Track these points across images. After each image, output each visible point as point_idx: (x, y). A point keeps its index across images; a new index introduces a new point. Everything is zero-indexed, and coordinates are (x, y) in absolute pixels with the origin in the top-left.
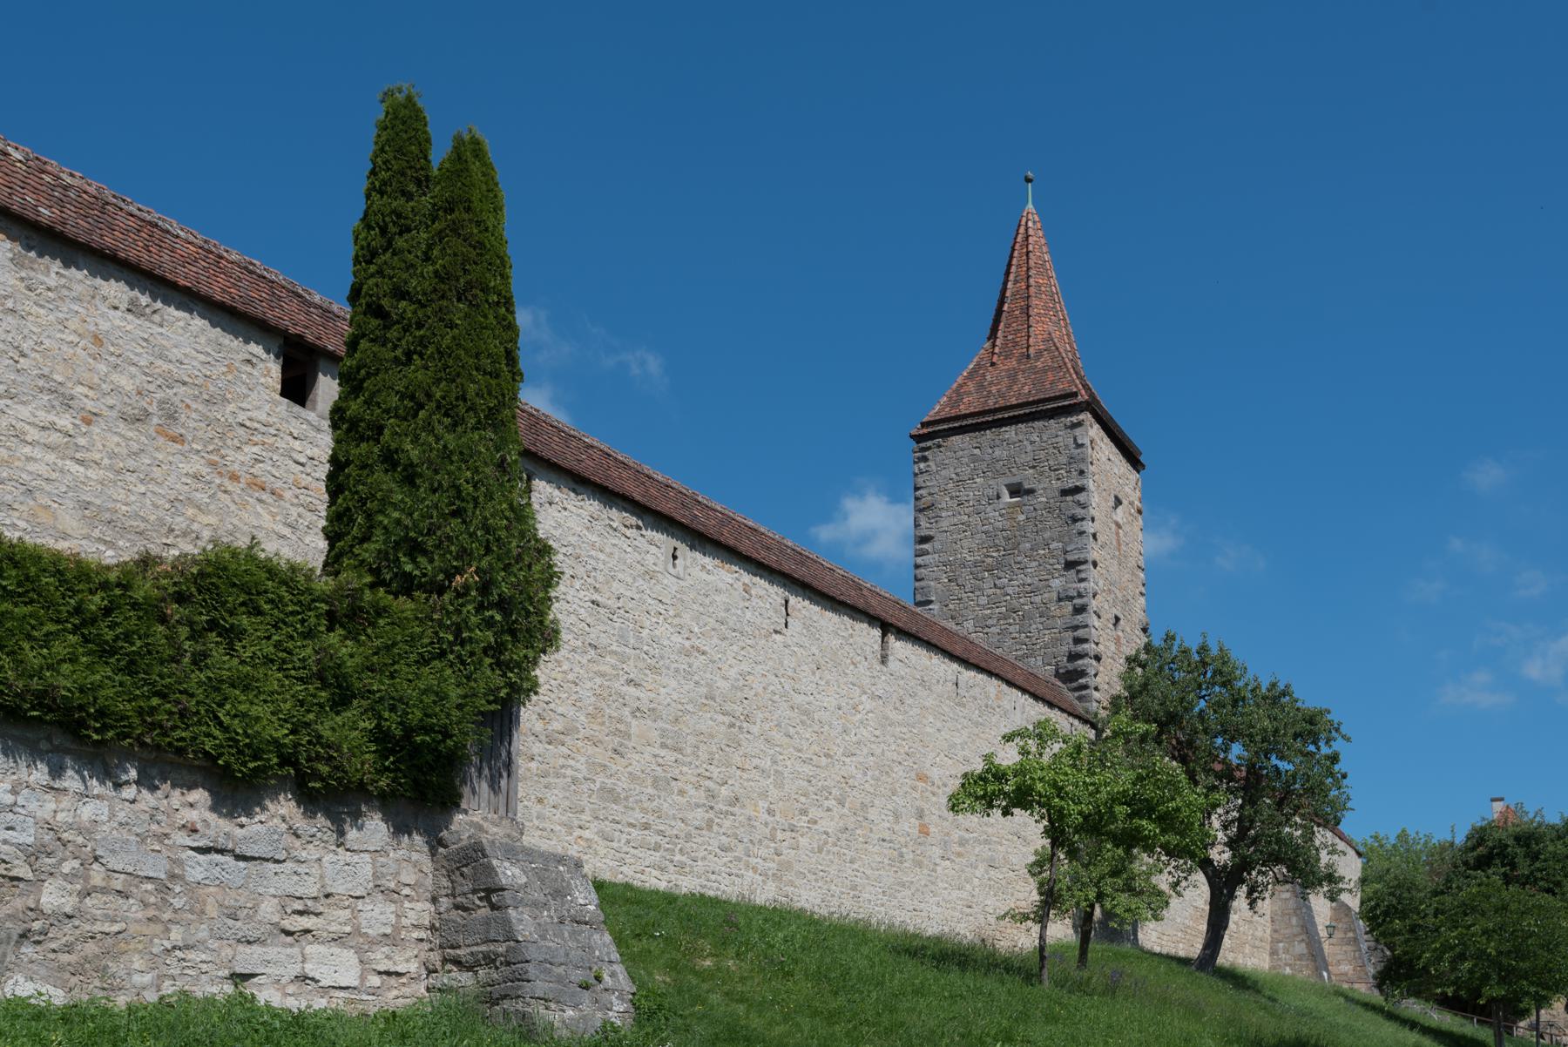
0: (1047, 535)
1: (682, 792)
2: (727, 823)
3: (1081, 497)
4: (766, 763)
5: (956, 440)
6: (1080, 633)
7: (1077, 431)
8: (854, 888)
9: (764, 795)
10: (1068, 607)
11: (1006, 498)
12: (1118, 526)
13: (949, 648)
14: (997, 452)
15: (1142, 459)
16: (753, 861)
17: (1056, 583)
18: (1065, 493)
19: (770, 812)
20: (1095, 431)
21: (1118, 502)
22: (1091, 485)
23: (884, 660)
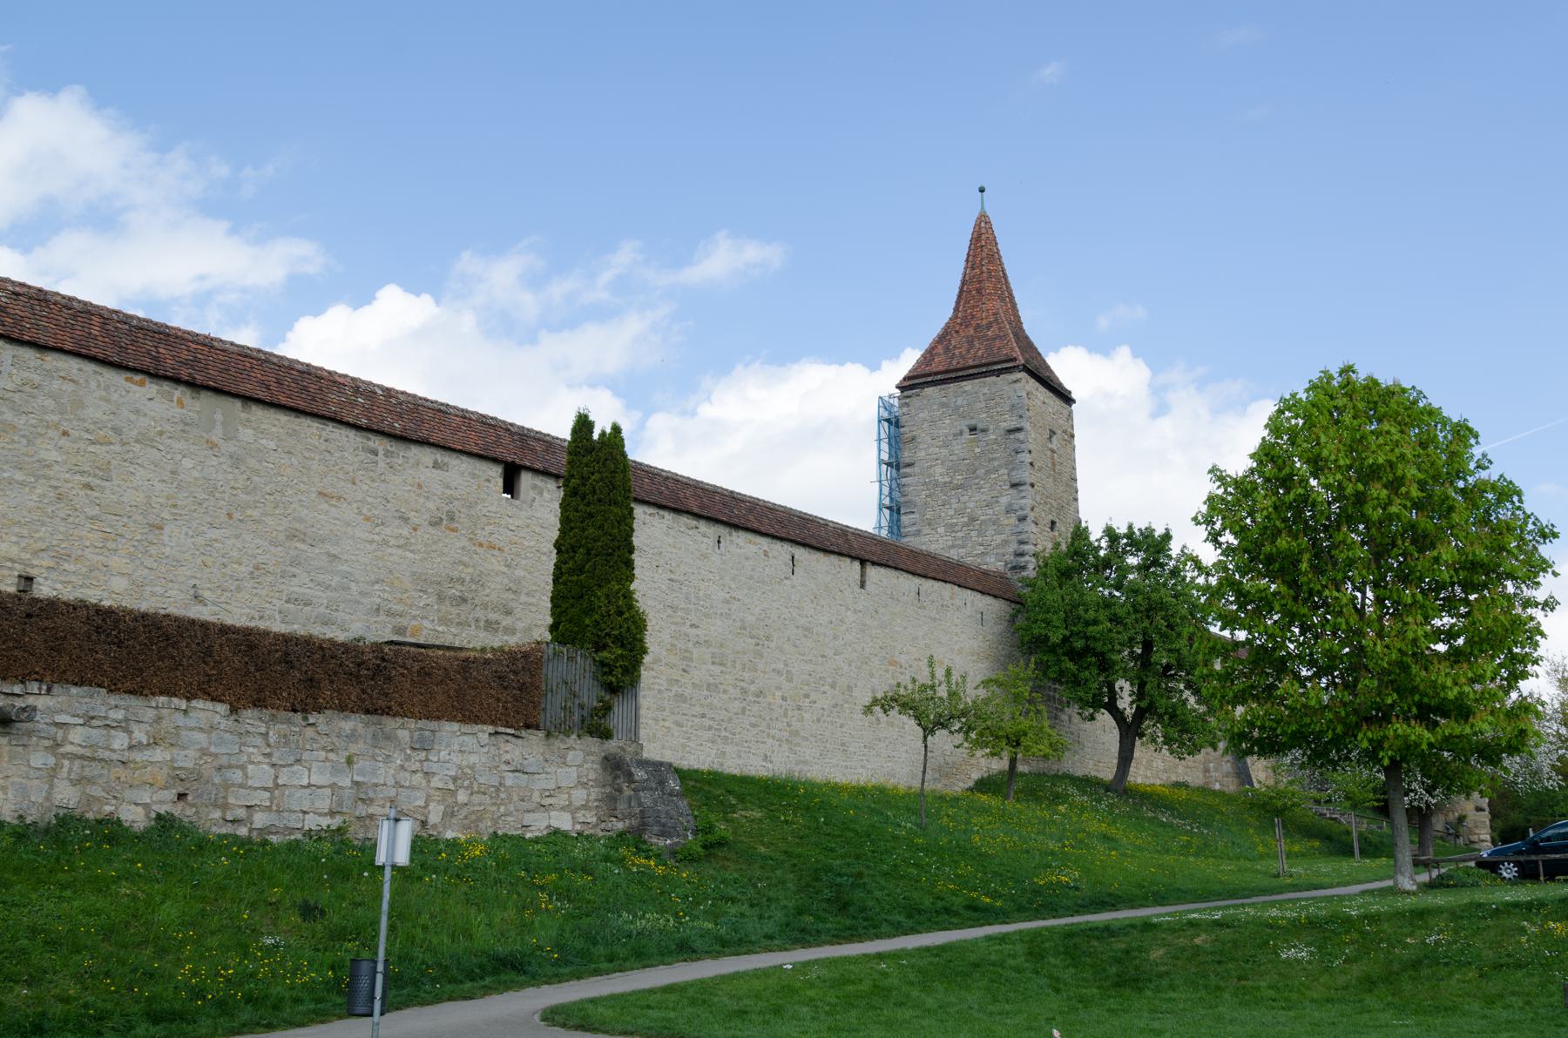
0: (996, 463)
1: (725, 692)
2: (755, 708)
3: (1021, 436)
4: (781, 666)
5: (929, 391)
6: (1023, 536)
7: (1017, 386)
8: (843, 744)
9: (779, 688)
10: (1013, 520)
11: (967, 435)
12: (1053, 451)
13: (911, 569)
14: (959, 402)
15: (1074, 396)
16: (773, 732)
17: (1004, 500)
18: (1010, 431)
19: (784, 699)
20: (1032, 384)
21: (1053, 433)
22: (1027, 426)
23: (863, 585)
